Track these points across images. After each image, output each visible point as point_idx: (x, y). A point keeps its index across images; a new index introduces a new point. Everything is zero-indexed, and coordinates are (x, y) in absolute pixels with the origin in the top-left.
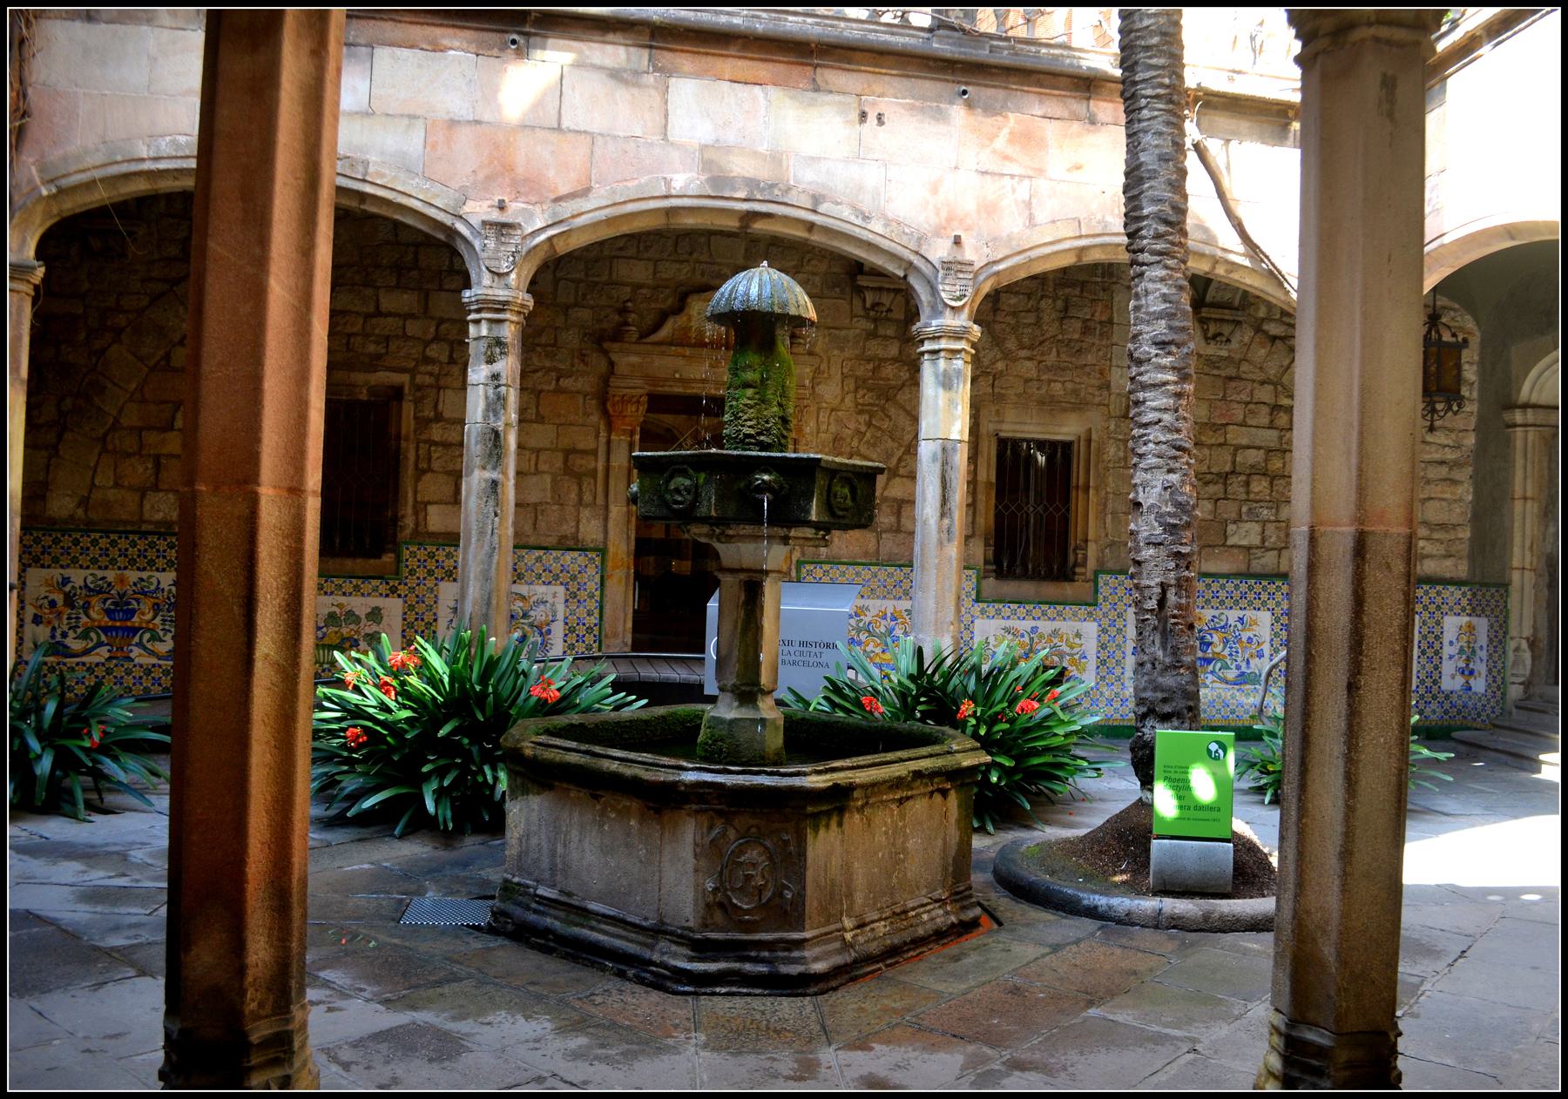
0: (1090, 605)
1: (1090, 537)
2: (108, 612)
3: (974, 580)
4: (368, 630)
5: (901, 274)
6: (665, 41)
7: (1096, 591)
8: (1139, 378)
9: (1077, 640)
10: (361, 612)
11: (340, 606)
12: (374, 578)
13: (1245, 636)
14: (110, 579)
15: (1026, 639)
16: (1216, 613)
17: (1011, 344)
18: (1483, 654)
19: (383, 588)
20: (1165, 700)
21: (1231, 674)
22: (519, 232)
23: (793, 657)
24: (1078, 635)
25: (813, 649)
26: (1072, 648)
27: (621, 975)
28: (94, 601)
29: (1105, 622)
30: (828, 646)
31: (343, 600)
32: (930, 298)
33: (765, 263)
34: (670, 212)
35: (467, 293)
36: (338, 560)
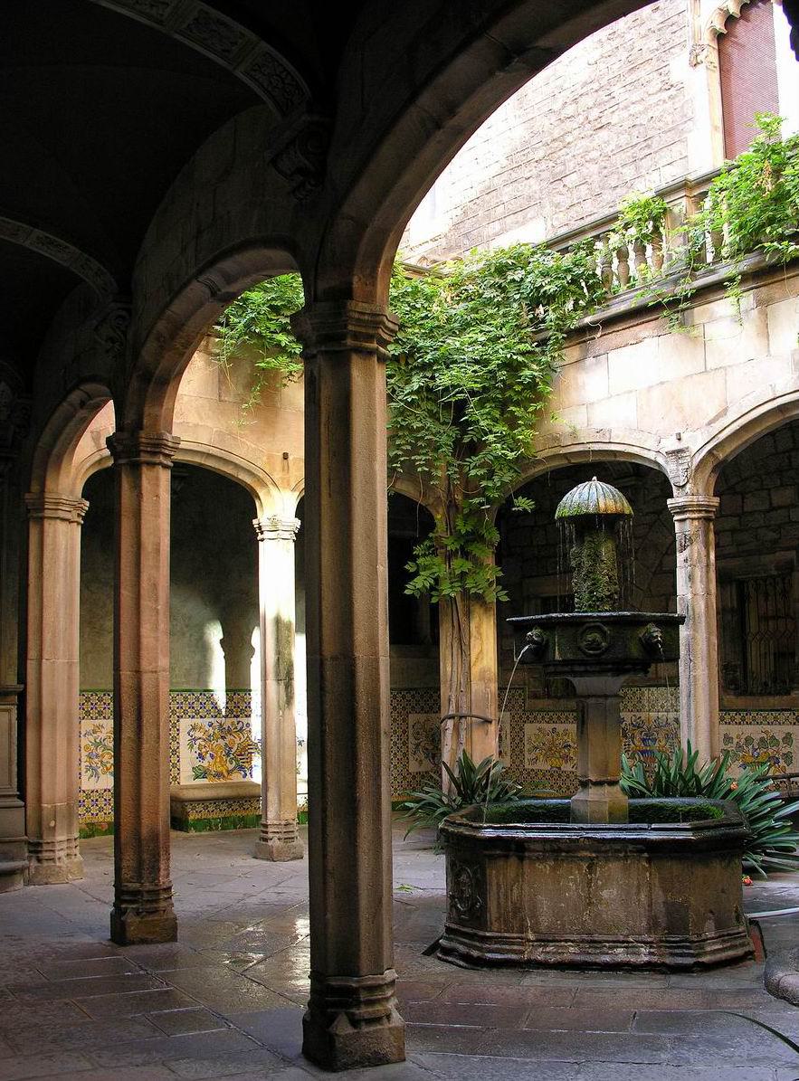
2: (644, 740)
4: (785, 751)
6: (773, 276)
10: (779, 737)
11: (766, 732)
12: (786, 710)
14: (643, 718)
19: (792, 718)
22: (687, 454)
28: (636, 733)
31: (768, 728)
33: (595, 478)
34: (782, 409)
35: (669, 501)
36: (765, 698)
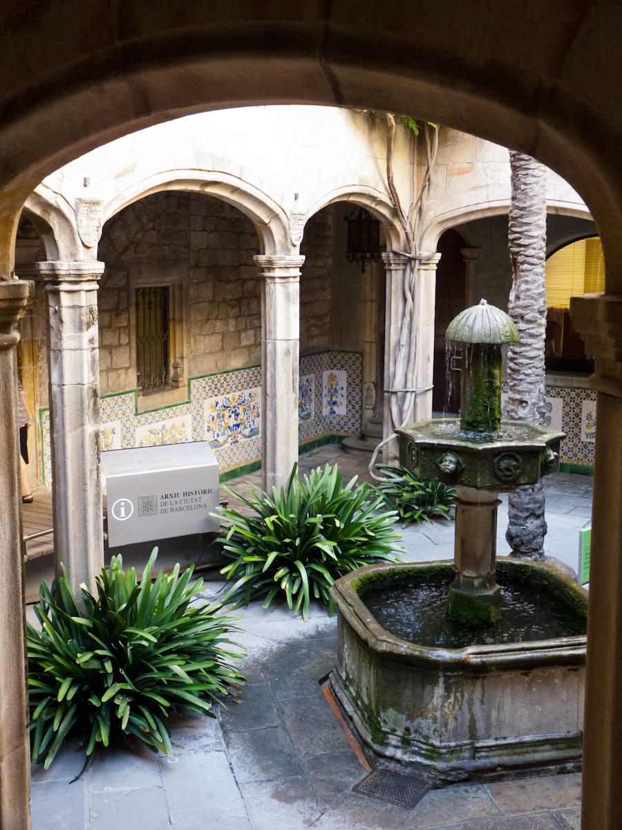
0: (187, 403)
1: (185, 355)
3: (134, 400)
5: (267, 221)
7: (189, 392)
8: (530, 331)
9: (183, 429)
13: (252, 404)
15: (160, 435)
16: (240, 393)
17: (144, 220)
18: (345, 392)
20: (540, 507)
21: (247, 432)
23: (179, 505)
24: (183, 425)
25: (194, 496)
26: (181, 435)
27: (563, 771)
29: (195, 412)
30: (205, 492)
32: (281, 239)
